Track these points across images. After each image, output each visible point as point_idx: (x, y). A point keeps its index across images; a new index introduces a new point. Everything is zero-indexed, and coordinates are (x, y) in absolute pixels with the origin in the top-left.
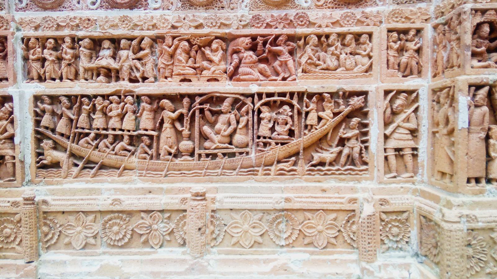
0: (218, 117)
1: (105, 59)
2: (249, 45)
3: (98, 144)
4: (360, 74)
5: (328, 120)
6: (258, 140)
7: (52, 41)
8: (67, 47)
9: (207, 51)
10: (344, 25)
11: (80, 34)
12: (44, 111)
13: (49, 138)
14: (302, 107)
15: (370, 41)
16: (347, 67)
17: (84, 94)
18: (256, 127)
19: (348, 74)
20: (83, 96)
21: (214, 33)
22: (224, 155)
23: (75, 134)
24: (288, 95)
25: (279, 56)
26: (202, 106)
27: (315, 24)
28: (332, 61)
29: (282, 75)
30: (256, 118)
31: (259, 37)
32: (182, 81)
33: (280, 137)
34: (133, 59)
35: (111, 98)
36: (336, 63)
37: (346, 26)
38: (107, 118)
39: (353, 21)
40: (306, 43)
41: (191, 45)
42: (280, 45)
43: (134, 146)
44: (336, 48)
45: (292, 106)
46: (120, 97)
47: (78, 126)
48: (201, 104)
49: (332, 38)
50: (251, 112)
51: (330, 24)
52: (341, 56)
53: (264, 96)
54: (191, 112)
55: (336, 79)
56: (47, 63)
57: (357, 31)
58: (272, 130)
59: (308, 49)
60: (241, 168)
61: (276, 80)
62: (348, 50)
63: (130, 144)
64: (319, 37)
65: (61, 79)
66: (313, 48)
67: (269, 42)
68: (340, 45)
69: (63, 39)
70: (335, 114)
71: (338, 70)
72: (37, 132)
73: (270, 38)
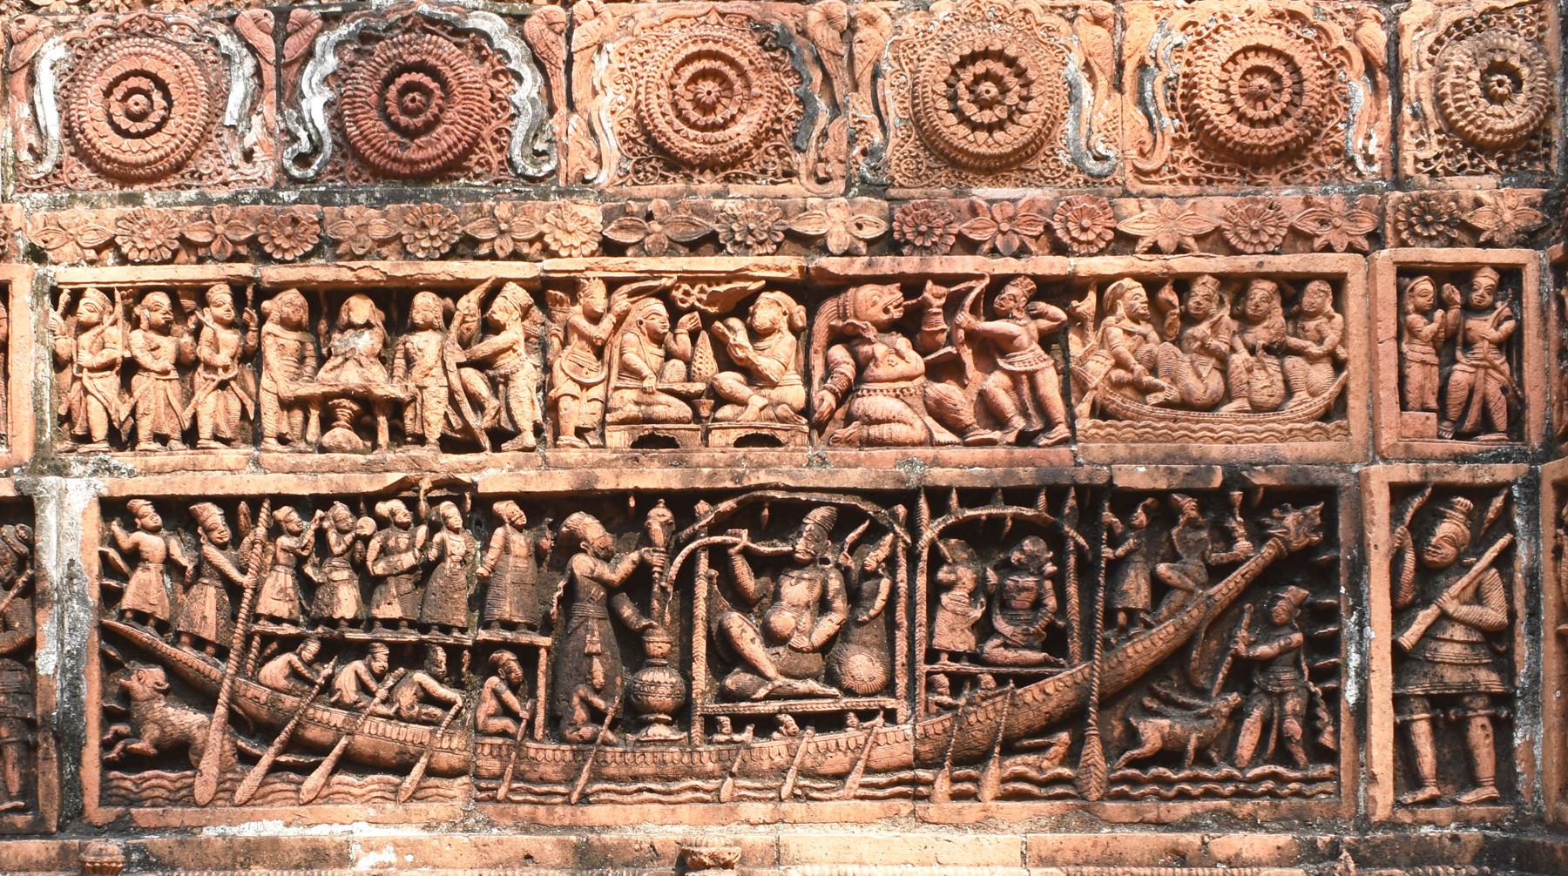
0: (775, 579)
1: (357, 364)
2: (897, 314)
3: (330, 679)
4: (1305, 426)
5: (1190, 592)
6: (928, 667)
7: (162, 299)
8: (218, 320)
9: (738, 334)
10: (1241, 246)
11: (271, 273)
12: (135, 557)
13: (149, 656)
14: (1095, 542)
15: (1338, 306)
16: (1257, 398)
17: (284, 492)
18: (921, 614)
19: (1260, 423)
20: (278, 500)
21: (761, 268)
22: (803, 720)
23: (248, 638)
24: (1042, 499)
25: (1003, 354)
26: (718, 539)
27: (1134, 240)
28: (1199, 376)
29: (1019, 423)
30: (921, 581)
31: (929, 284)
32: (640, 443)
33: (1011, 655)
34: (460, 366)
35: (382, 508)
36: (1215, 382)
37: (1250, 249)
38: (370, 585)
39: (1272, 231)
40: (1103, 311)
41: (675, 313)
42: (1005, 315)
43: (458, 685)
44: (1215, 327)
45: (1056, 541)
46: (411, 504)
47: (261, 610)
48: (716, 528)
49: (1200, 290)
50: (902, 561)
51: (1191, 241)
52: (1234, 356)
53: (954, 500)
54: (679, 559)
55: (1215, 440)
56: (139, 381)
57: (1288, 269)
58: (984, 629)
59: (1115, 328)
60: (869, 770)
61: (991, 443)
62: (1259, 335)
63: (453, 678)
64: (1151, 284)
65: (190, 436)
66: (1128, 324)
67: (969, 301)
68: (1227, 318)
69: (199, 292)
70: (1218, 572)
71: (1226, 409)
72: (106, 633)
73: (971, 289)
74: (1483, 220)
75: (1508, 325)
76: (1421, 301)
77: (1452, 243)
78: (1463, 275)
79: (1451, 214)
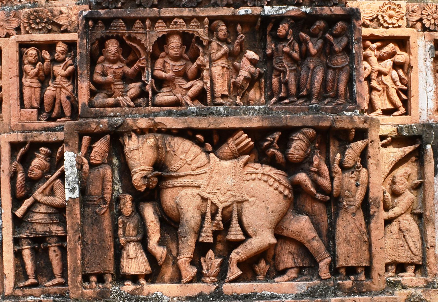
74: (62, 21)
75: (70, 68)
76: (30, 58)
77: (50, 31)
78: (51, 46)
79: (48, 18)
